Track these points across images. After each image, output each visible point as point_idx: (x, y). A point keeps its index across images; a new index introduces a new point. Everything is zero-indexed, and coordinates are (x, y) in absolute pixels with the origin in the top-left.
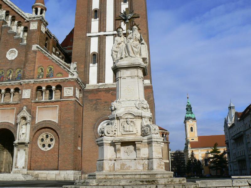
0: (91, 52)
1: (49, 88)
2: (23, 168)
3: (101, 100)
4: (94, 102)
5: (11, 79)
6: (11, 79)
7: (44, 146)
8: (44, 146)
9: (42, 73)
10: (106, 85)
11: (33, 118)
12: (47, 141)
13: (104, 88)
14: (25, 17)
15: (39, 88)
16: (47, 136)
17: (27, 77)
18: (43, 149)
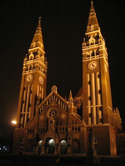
1: (76, 128)
7: (76, 146)
8: (76, 146)
10: (94, 125)
11: (72, 137)
12: (77, 144)
16: (77, 143)
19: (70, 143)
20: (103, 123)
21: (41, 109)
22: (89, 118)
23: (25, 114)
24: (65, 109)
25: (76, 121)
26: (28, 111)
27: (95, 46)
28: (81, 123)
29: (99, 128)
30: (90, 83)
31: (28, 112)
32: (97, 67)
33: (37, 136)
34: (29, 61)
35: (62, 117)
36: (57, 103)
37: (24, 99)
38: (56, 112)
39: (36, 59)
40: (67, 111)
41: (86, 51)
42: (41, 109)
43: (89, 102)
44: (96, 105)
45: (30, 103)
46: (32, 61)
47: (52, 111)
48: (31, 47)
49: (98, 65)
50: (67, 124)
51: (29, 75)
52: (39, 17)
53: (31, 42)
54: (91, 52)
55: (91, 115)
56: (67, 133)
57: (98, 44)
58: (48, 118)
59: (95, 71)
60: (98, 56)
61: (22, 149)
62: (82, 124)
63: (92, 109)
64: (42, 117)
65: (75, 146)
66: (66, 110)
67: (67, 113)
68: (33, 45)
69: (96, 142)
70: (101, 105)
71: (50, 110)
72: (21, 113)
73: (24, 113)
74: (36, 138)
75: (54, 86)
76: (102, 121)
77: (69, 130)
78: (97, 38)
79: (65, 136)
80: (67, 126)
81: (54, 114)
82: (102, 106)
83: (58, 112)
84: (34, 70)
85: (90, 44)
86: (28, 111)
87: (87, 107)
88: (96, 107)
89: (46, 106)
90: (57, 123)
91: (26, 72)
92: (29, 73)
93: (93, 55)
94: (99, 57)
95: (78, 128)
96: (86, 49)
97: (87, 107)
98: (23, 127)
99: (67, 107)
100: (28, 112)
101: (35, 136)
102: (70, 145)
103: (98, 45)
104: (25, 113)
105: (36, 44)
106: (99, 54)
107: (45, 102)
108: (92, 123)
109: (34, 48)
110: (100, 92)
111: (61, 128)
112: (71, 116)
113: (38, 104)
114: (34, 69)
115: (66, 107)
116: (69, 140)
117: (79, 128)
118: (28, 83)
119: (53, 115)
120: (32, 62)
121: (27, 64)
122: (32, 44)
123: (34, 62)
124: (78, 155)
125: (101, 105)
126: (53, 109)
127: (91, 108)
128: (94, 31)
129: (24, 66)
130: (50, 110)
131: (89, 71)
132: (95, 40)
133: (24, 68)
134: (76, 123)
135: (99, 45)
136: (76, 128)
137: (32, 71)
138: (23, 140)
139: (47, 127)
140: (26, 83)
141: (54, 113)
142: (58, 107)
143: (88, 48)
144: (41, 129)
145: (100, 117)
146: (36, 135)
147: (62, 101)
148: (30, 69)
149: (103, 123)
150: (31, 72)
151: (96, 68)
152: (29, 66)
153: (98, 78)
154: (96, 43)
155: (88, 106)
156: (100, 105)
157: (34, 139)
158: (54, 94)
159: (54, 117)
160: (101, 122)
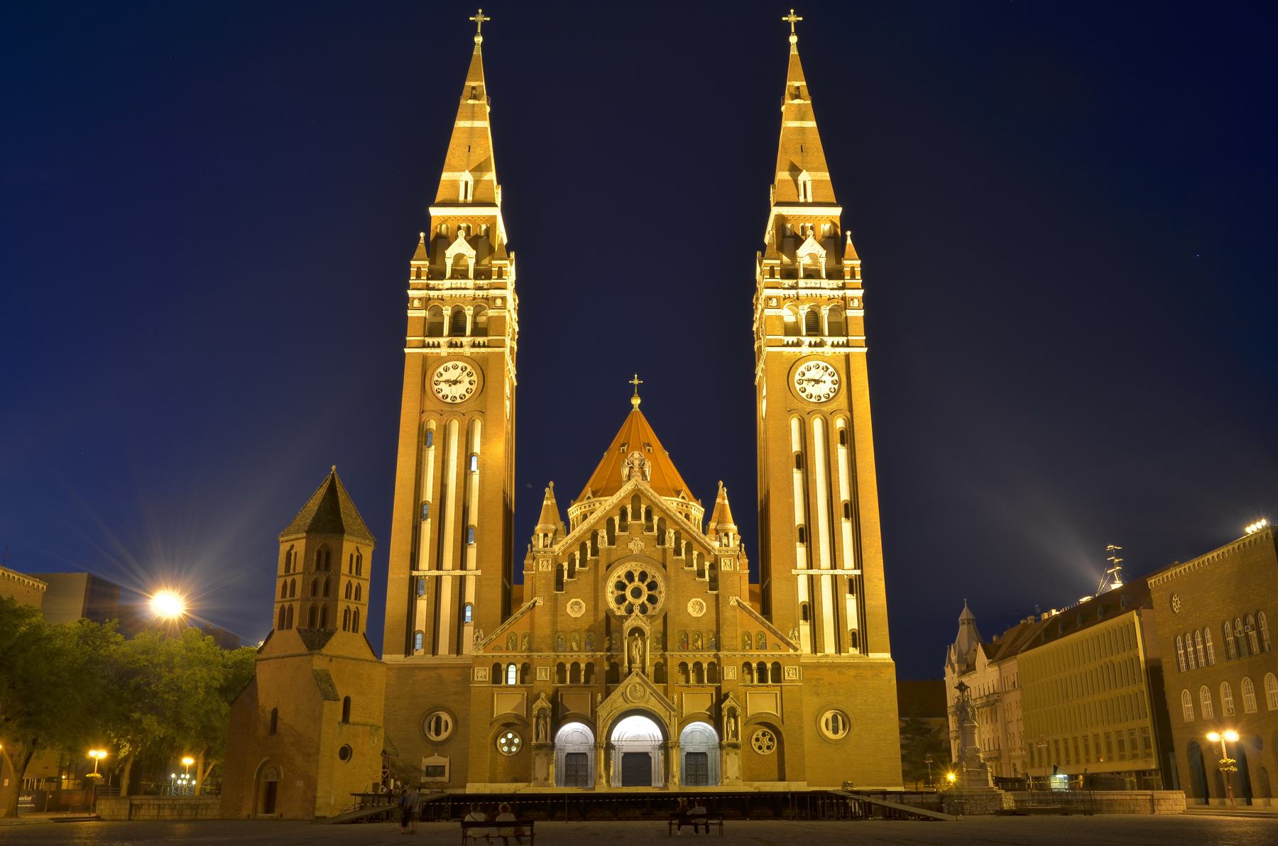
0: (800, 601)
1: (762, 667)
2: (737, 778)
3: (822, 679)
4: (814, 683)
5: (700, 647)
6: (700, 647)
7: (760, 748)
9: (749, 642)
10: (827, 656)
12: (766, 741)
13: (826, 662)
14: (710, 548)
15: (747, 665)
16: (764, 735)
17: (727, 647)
18: (760, 752)
19: (735, 734)
20: (865, 650)
21: (566, 565)
22: (801, 622)
23: (438, 580)
24: (701, 573)
25: (763, 635)
26: (462, 563)
27: (827, 289)
28: (783, 645)
29: (853, 672)
30: (802, 461)
31: (459, 573)
32: (837, 392)
33: (554, 700)
34: (447, 283)
35: (690, 610)
36: (661, 539)
37: (429, 495)
38: (652, 586)
39: (494, 280)
40: (714, 584)
41: (781, 302)
42: (566, 565)
43: (801, 550)
44: (834, 566)
45: (474, 519)
46: (470, 283)
47: (630, 576)
48: (441, 195)
49: (839, 382)
50: (718, 647)
51: (450, 364)
52: (475, 14)
53: (437, 164)
54: (804, 310)
55: (810, 612)
56: (718, 690)
57: (840, 282)
58: (612, 611)
59: (825, 409)
60: (842, 340)
61: (438, 771)
62: (791, 651)
63: (812, 582)
64: (576, 603)
65: (756, 749)
66: (707, 578)
67: (717, 596)
68: (454, 184)
69: (836, 731)
70: (858, 572)
71: (620, 572)
72: (415, 573)
73: (435, 573)
74: (549, 713)
75: (636, 455)
76: (860, 640)
77: (731, 673)
78: (834, 244)
79: (704, 702)
80: (716, 656)
81: (644, 598)
82: (861, 577)
83: (667, 587)
84: (481, 340)
85: (801, 274)
86: (462, 563)
87: (794, 572)
88: (835, 579)
89: (595, 552)
90: (663, 641)
91: (430, 340)
92: (452, 350)
93: (814, 327)
94: (847, 345)
95: (769, 666)
96: (780, 293)
97: (794, 572)
98: (434, 651)
99: (714, 567)
100: (459, 573)
101: (543, 703)
102: (735, 746)
103: (840, 288)
104: (440, 573)
105: (477, 182)
106: (847, 335)
107: (588, 530)
108: (816, 645)
109: (465, 205)
110: (852, 510)
111: (683, 666)
112: (733, 607)
113: (550, 535)
114: (478, 331)
115: (707, 564)
116: (733, 721)
117: (777, 668)
118: (451, 407)
119: (640, 601)
120: (470, 293)
121: (432, 293)
122: (445, 176)
123: (480, 293)
124: (780, 787)
125: (858, 572)
126: (637, 569)
127: (811, 579)
128: (814, 204)
129: (416, 303)
130: (620, 572)
131: (796, 404)
132: (822, 252)
133: (415, 314)
134: (764, 647)
135: (843, 287)
136: (762, 667)
137: (474, 346)
138: (438, 719)
139: (608, 659)
140: (429, 405)
141: (644, 587)
142: (668, 565)
143: (792, 288)
144: (575, 666)
145: (852, 623)
146: (547, 695)
147: (684, 534)
148: (457, 329)
149: (865, 650)
150: (467, 351)
151: (832, 395)
152: (447, 312)
153: (839, 445)
154: (830, 276)
155: (796, 568)
156: (848, 567)
157: (538, 718)
158: (636, 497)
159: (643, 609)
160: (855, 645)
